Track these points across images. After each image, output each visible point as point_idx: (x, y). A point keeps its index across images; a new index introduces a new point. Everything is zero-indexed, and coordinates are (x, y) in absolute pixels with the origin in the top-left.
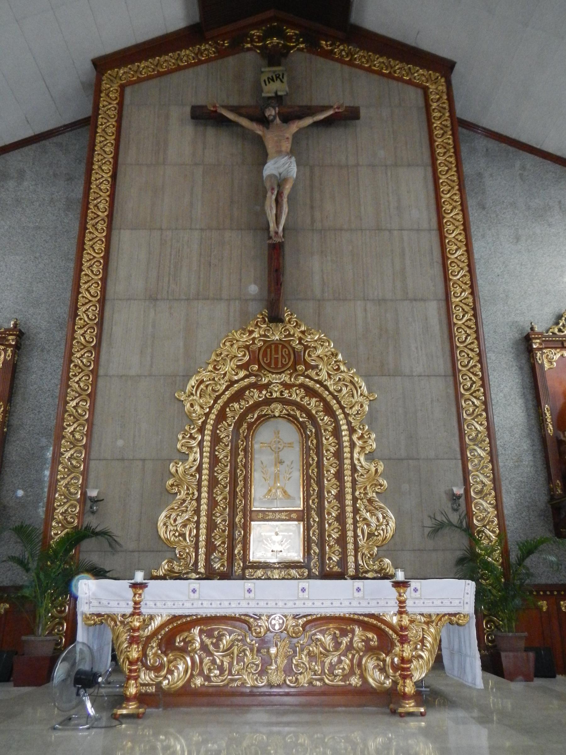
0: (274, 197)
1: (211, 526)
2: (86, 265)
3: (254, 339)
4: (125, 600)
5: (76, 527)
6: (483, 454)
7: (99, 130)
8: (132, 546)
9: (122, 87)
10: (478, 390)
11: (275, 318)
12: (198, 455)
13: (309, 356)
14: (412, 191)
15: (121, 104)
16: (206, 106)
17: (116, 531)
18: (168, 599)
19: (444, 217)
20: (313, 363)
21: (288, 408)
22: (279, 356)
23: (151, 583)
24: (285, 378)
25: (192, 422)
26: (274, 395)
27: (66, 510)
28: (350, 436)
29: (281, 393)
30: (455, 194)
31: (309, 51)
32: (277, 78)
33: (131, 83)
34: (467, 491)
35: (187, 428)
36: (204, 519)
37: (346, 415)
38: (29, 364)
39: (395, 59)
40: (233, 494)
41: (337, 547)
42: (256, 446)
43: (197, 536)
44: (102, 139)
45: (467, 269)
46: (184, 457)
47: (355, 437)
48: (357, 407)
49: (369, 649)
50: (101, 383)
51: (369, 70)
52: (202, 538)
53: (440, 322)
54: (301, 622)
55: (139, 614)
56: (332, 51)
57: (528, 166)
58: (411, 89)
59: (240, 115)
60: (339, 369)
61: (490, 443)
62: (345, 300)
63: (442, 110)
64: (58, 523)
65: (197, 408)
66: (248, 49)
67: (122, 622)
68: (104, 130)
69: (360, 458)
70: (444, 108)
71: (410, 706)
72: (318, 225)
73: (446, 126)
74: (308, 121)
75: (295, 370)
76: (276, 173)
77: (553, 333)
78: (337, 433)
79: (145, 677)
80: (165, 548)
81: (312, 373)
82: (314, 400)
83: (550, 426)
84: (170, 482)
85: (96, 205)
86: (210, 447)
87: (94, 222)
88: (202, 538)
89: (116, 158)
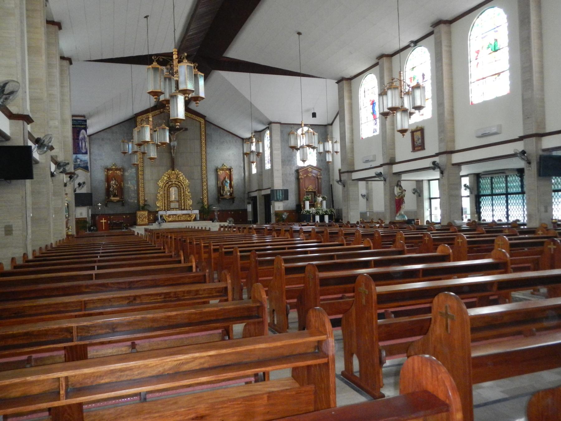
14: (197, 142)
18: (169, 213)
80: (158, 207)
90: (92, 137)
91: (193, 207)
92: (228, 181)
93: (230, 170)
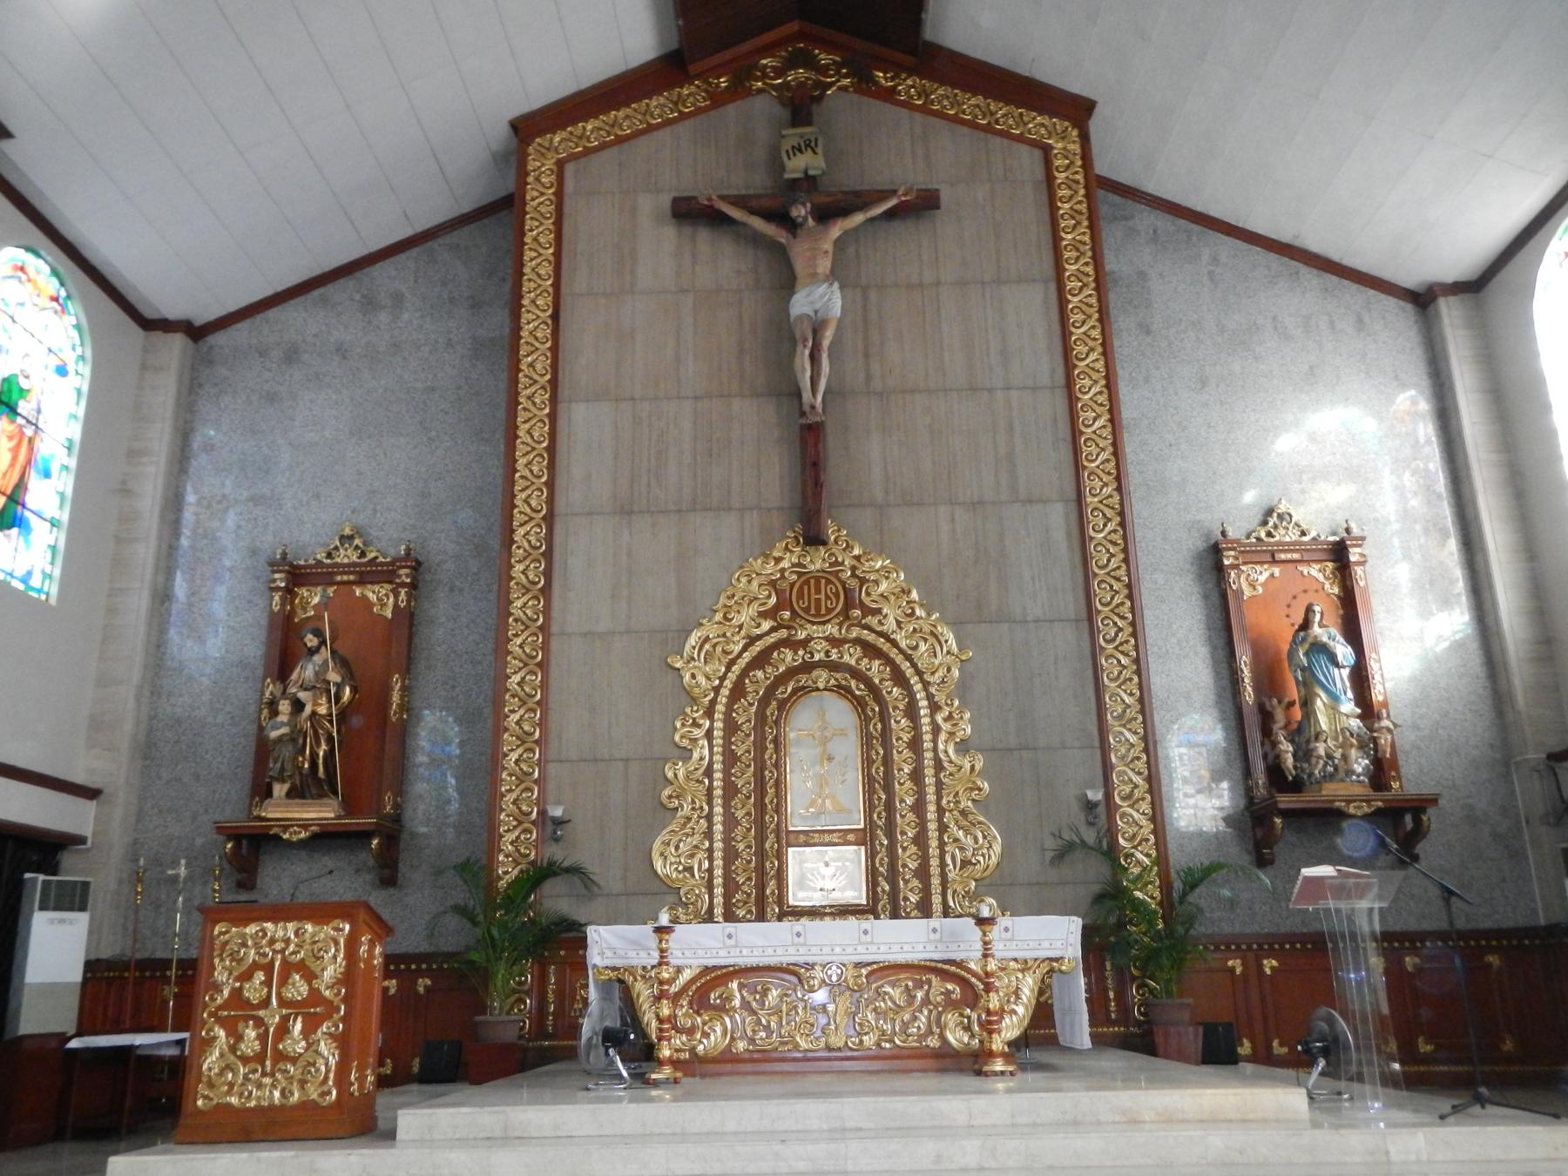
0: (807, 352)
1: (730, 855)
2: (522, 461)
3: (783, 570)
4: (647, 949)
5: (533, 863)
6: (1133, 739)
7: (528, 240)
8: (617, 887)
9: (560, 164)
10: (1127, 642)
11: (814, 539)
12: (706, 752)
13: (868, 594)
15: (559, 194)
16: (695, 198)
17: (593, 867)
18: (700, 945)
19: (1075, 366)
20: (874, 606)
21: (838, 676)
22: (823, 597)
23: (678, 927)
24: (831, 629)
25: (694, 700)
26: (817, 657)
27: (518, 837)
28: (932, 715)
29: (827, 653)
30: (1093, 327)
31: (859, 91)
32: (808, 146)
33: (574, 157)
34: (1108, 796)
35: (688, 710)
36: (718, 845)
37: (926, 685)
38: (433, 612)
39: (997, 98)
40: (761, 807)
41: (915, 883)
42: (792, 735)
43: (710, 870)
44: (534, 254)
45: (1111, 449)
46: (685, 755)
47: (939, 718)
48: (940, 673)
49: (950, 1004)
50: (555, 645)
51: (955, 120)
52: (718, 872)
53: (1069, 534)
54: (864, 971)
55: (667, 964)
56: (893, 91)
57: (1223, 259)
58: (1023, 149)
59: (752, 212)
60: (913, 613)
61: (1144, 722)
62: (920, 504)
63: (1074, 186)
64: (507, 856)
65: (701, 680)
66: (760, 91)
67: (643, 977)
68: (535, 239)
69: (947, 749)
70: (1077, 182)
71: (999, 1066)
72: (877, 384)
73: (1080, 213)
74: (858, 218)
75: (847, 617)
76: (808, 310)
77: (1259, 539)
78: (912, 712)
79: (679, 1041)
80: (667, 892)
81: (872, 621)
82: (877, 662)
83: (1249, 689)
84: (667, 792)
85: (531, 365)
86: (723, 738)
87: (528, 392)
88: (718, 872)
89: (557, 286)
90: (219, 339)
91: (1018, 892)
92: (1344, 652)
93: (1339, 554)
